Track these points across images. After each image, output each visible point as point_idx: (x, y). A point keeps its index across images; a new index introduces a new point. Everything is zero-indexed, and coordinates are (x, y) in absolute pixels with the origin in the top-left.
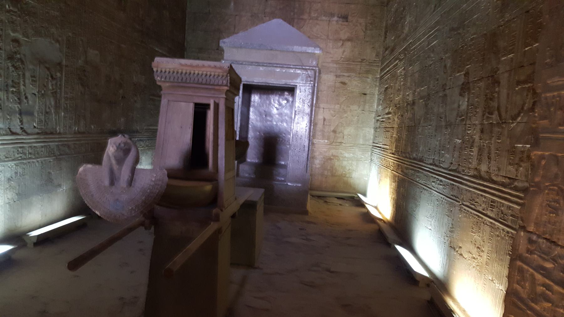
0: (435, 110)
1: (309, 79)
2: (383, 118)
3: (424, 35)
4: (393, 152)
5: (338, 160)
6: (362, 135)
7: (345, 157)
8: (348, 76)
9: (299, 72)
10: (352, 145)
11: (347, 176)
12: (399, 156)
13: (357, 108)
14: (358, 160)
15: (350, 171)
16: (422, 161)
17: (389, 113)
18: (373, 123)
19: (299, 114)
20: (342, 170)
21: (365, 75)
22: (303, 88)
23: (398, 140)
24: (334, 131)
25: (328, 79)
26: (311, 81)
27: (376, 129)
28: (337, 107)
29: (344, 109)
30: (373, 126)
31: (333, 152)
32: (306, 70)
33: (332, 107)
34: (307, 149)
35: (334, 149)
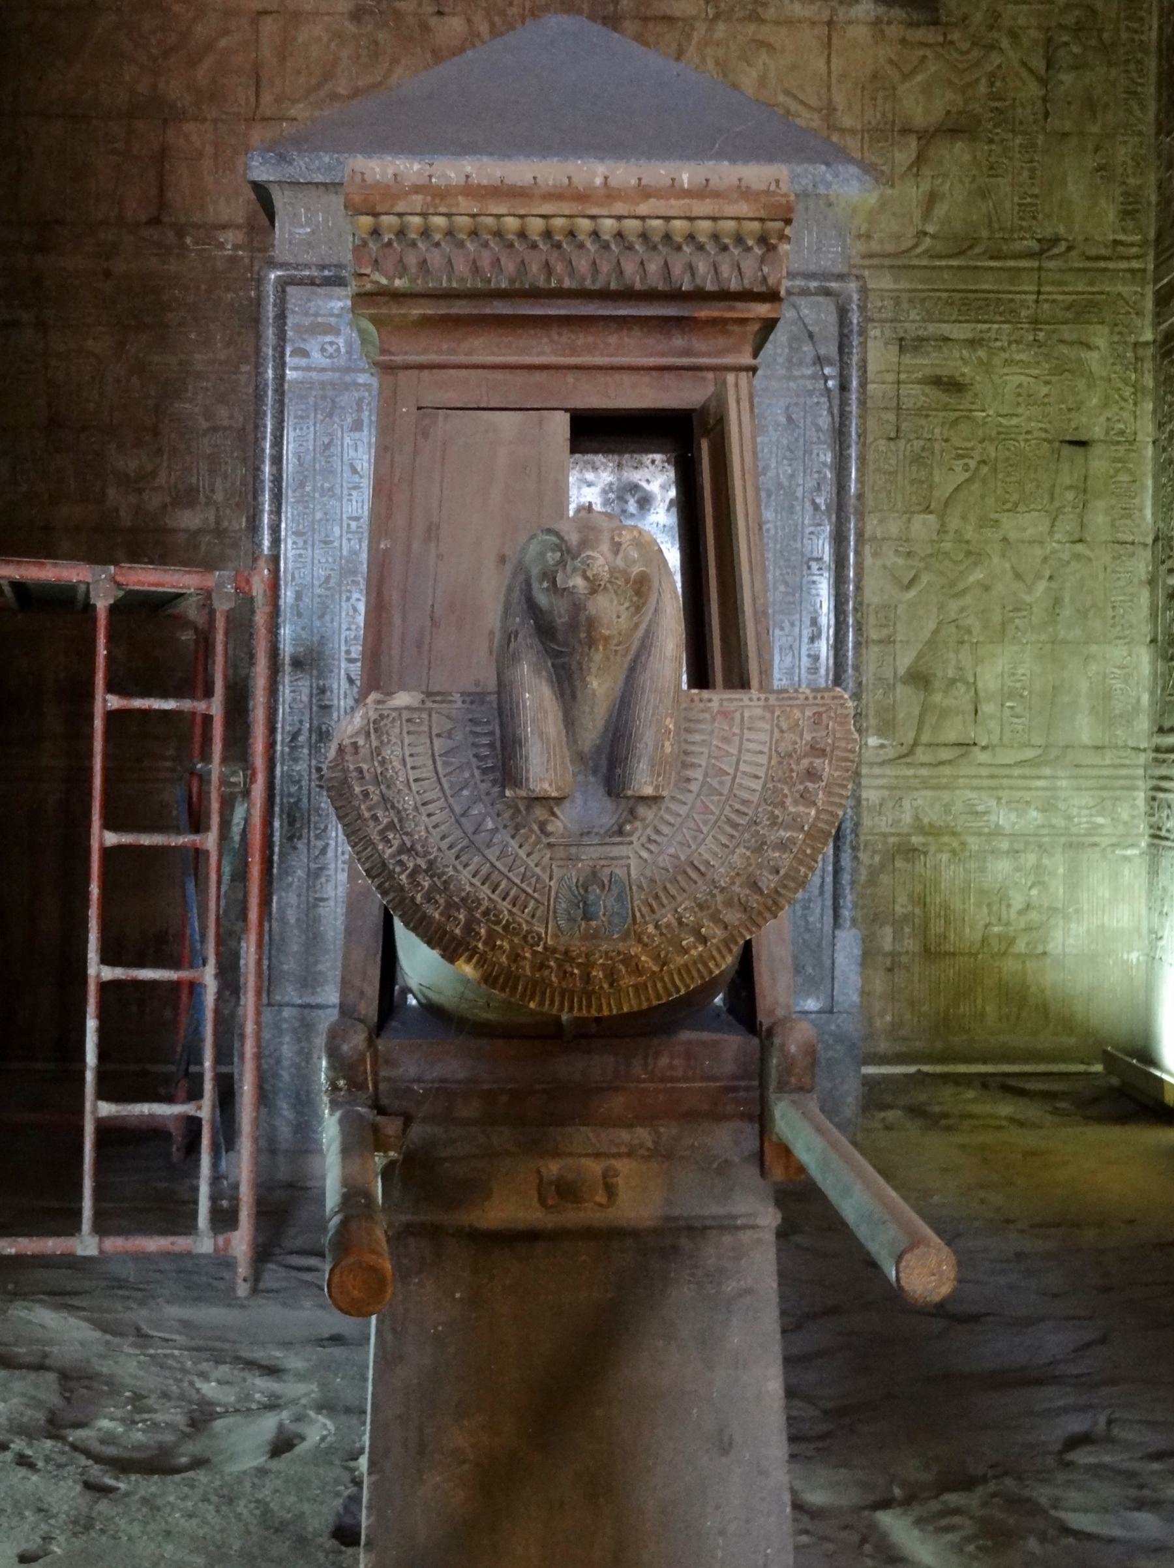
1: (807, 348)
6: (1084, 686)
7: (997, 832)
8: (973, 343)
10: (1029, 754)
11: (1021, 946)
13: (1044, 526)
14: (1075, 845)
15: (1033, 916)
18: (1145, 612)
20: (983, 916)
21: (1067, 332)
24: (919, 678)
26: (820, 361)
28: (922, 526)
29: (959, 539)
30: (1146, 629)
35: (925, 785)
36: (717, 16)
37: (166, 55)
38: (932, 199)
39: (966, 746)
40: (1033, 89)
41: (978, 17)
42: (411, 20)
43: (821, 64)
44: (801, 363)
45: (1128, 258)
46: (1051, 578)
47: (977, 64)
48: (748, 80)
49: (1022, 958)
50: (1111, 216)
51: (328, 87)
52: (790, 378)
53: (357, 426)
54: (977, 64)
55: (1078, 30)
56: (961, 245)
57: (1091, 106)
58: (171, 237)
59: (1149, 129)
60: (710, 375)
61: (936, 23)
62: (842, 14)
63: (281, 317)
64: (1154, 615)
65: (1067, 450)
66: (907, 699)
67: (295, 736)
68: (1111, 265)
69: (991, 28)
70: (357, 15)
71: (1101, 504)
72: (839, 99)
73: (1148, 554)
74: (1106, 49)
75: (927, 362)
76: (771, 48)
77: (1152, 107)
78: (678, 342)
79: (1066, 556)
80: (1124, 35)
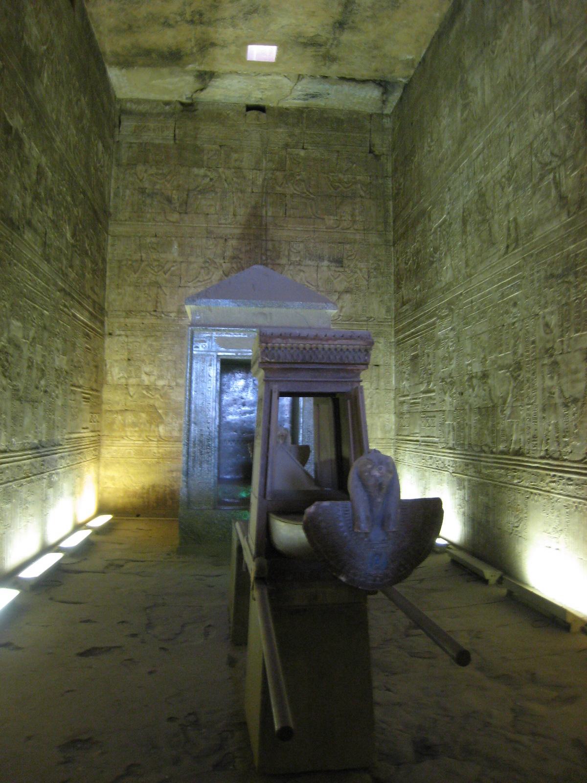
0: (538, 383)
2: (416, 399)
3: (491, 283)
4: (450, 445)
6: (379, 424)
12: (465, 450)
16: (522, 455)
17: (433, 391)
18: (393, 406)
23: (460, 428)
27: (400, 415)
30: (393, 410)
37: (158, 272)
40: (365, 283)
41: (352, 265)
42: (218, 264)
43: (315, 275)
45: (388, 322)
47: (352, 276)
50: (383, 311)
51: (198, 279)
53: (210, 365)
54: (352, 276)
55: (375, 269)
58: (158, 315)
59: (392, 292)
60: (350, 384)
61: (342, 267)
62: (320, 265)
63: (192, 339)
64: (395, 407)
65: (374, 367)
67: (194, 442)
68: (384, 324)
69: (355, 268)
70: (205, 262)
71: (382, 380)
72: (320, 284)
73: (393, 392)
74: (382, 273)
76: (304, 271)
77: (393, 286)
78: (342, 374)
79: (374, 392)
80: (386, 270)
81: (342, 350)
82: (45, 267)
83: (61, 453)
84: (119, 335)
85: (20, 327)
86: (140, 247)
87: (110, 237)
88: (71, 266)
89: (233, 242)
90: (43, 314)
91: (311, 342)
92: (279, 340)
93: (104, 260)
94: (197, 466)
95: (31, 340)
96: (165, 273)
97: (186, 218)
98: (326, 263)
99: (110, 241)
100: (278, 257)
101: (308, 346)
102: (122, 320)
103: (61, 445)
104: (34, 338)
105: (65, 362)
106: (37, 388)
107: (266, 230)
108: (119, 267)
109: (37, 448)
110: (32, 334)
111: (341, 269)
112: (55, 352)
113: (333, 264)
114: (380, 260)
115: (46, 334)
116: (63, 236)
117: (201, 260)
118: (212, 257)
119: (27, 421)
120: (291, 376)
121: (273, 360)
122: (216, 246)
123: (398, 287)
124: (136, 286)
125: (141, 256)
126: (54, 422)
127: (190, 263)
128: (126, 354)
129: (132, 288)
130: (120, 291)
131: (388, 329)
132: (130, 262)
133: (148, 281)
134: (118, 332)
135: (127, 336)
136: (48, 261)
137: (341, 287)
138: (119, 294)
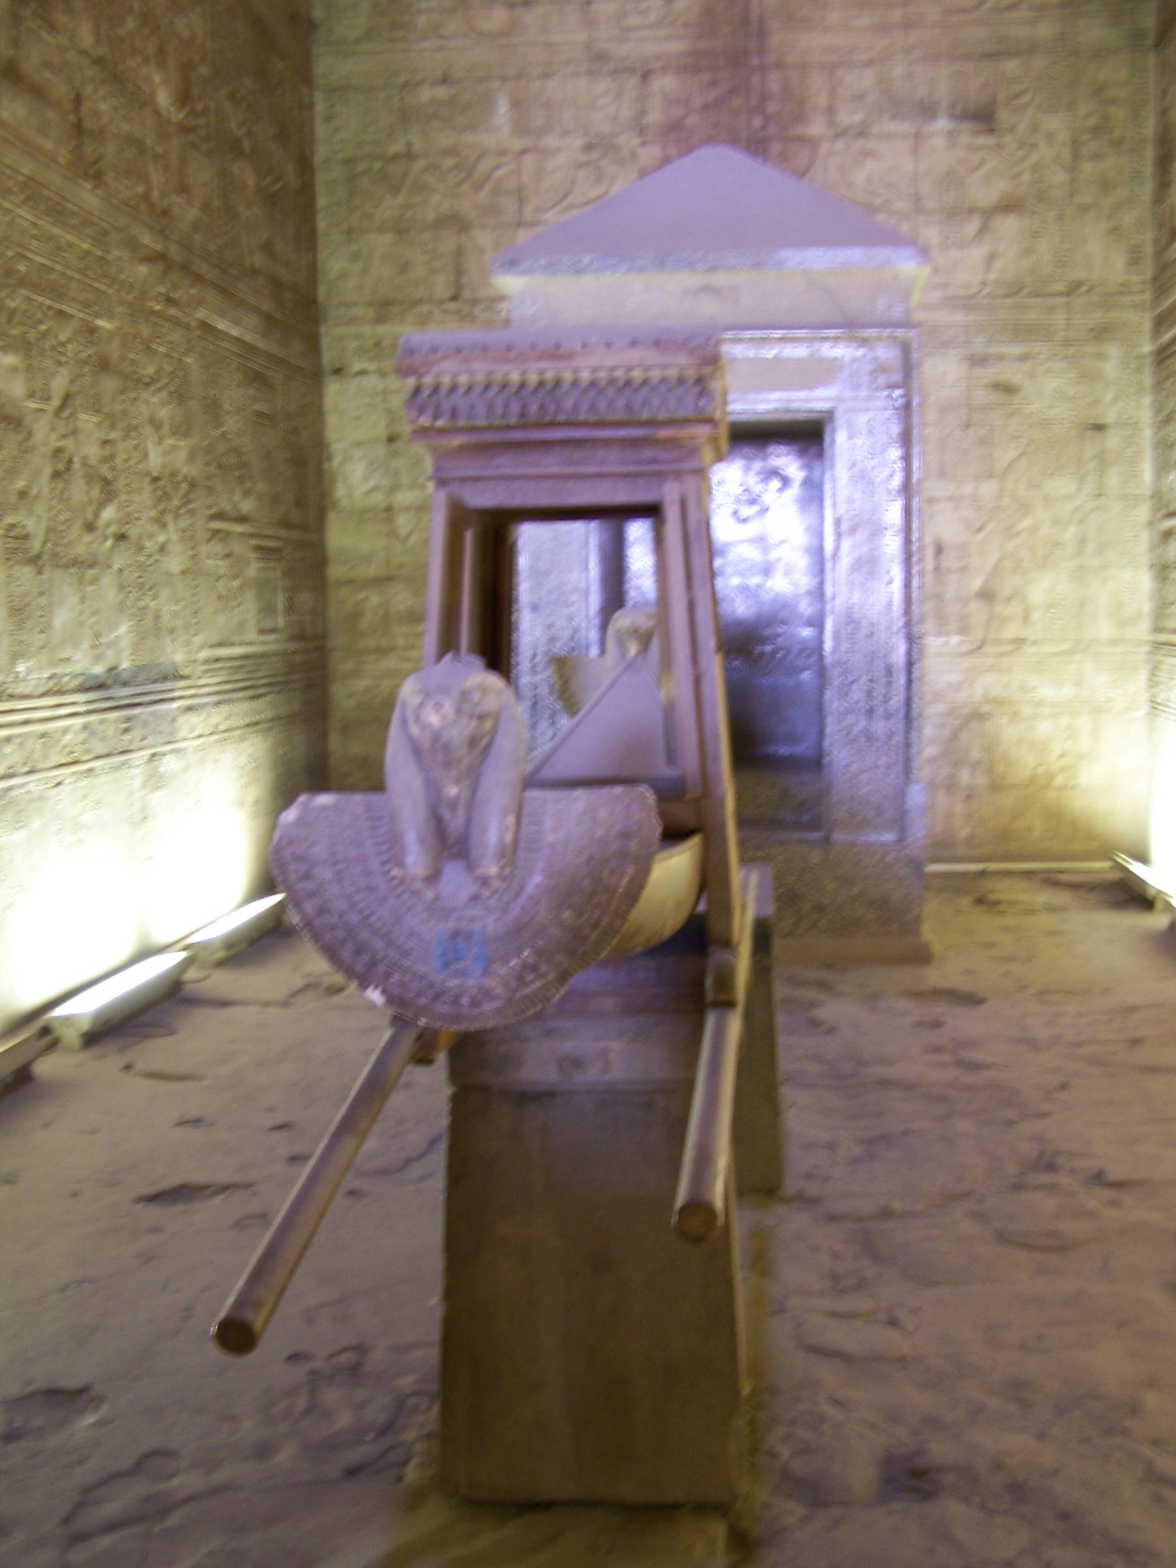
5: (1015, 716)
7: (1040, 703)
8: (1023, 358)
9: (830, 351)
11: (1058, 781)
19: (853, 530)
21: (1091, 349)
22: (862, 420)
24: (987, 595)
25: (943, 373)
26: (891, 387)
28: (988, 489)
31: (986, 684)
32: (863, 342)
33: (968, 489)
34: (900, 680)
36: (837, 136)
38: (991, 258)
39: (1020, 642)
40: (1061, 177)
44: (877, 389)
46: (1081, 522)
48: (859, 178)
49: (1062, 788)
52: (869, 398)
54: (1022, 160)
56: (1014, 289)
57: (1106, 186)
61: (991, 131)
64: (1152, 548)
65: (1089, 433)
66: (977, 611)
70: (589, 148)
74: (1117, 144)
75: (992, 373)
78: (648, 453)
81: (628, 383)
82: (88, 198)
83: (181, 698)
84: (362, 373)
85: (14, 370)
86: (405, 117)
87: (318, 96)
88: (183, 189)
89: (664, 83)
90: (93, 330)
91: (541, 365)
92: (450, 365)
93: (305, 165)
94: (544, 724)
95: (56, 402)
96: (478, 187)
97: (530, 17)
98: (942, 124)
99: (320, 108)
100: (799, 117)
101: (533, 378)
102: (367, 329)
103: (182, 677)
104: (67, 398)
105: (183, 454)
106: (90, 527)
107: (762, 34)
108: (352, 180)
109: (101, 686)
110: (59, 383)
111: (988, 140)
112: (148, 430)
113: (965, 126)
114: (1112, 102)
115: (110, 384)
116: (142, 101)
117: (578, 142)
118: (606, 128)
119: (61, 618)
120: (505, 464)
121: (440, 423)
122: (619, 96)
123: (1163, 186)
124: (401, 229)
125: (409, 145)
126: (157, 618)
127: (546, 153)
128: (383, 423)
129: (388, 238)
130: (354, 247)
131: (1131, 316)
132: (378, 165)
133: (431, 215)
134: (357, 366)
135: (382, 373)
136: (97, 178)
137: (986, 193)
138: (355, 257)
